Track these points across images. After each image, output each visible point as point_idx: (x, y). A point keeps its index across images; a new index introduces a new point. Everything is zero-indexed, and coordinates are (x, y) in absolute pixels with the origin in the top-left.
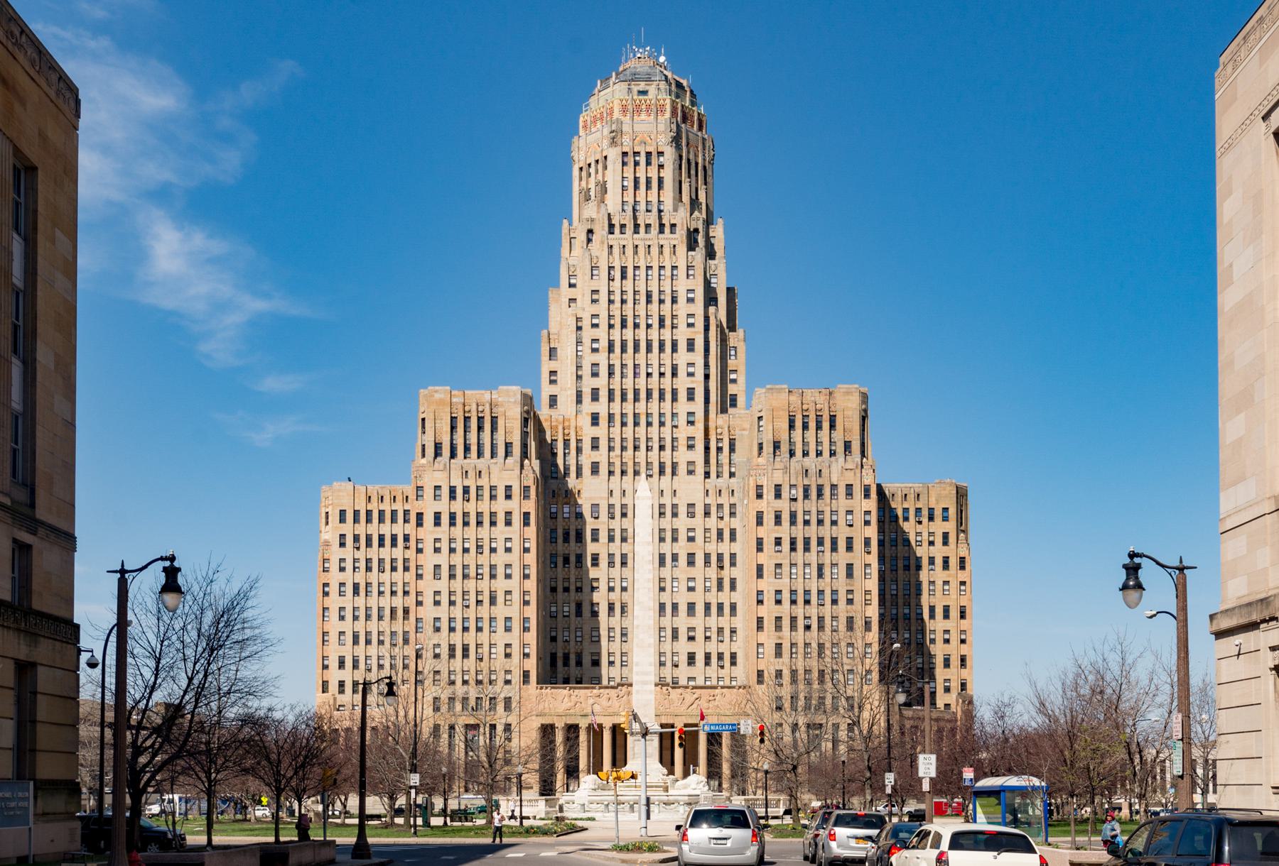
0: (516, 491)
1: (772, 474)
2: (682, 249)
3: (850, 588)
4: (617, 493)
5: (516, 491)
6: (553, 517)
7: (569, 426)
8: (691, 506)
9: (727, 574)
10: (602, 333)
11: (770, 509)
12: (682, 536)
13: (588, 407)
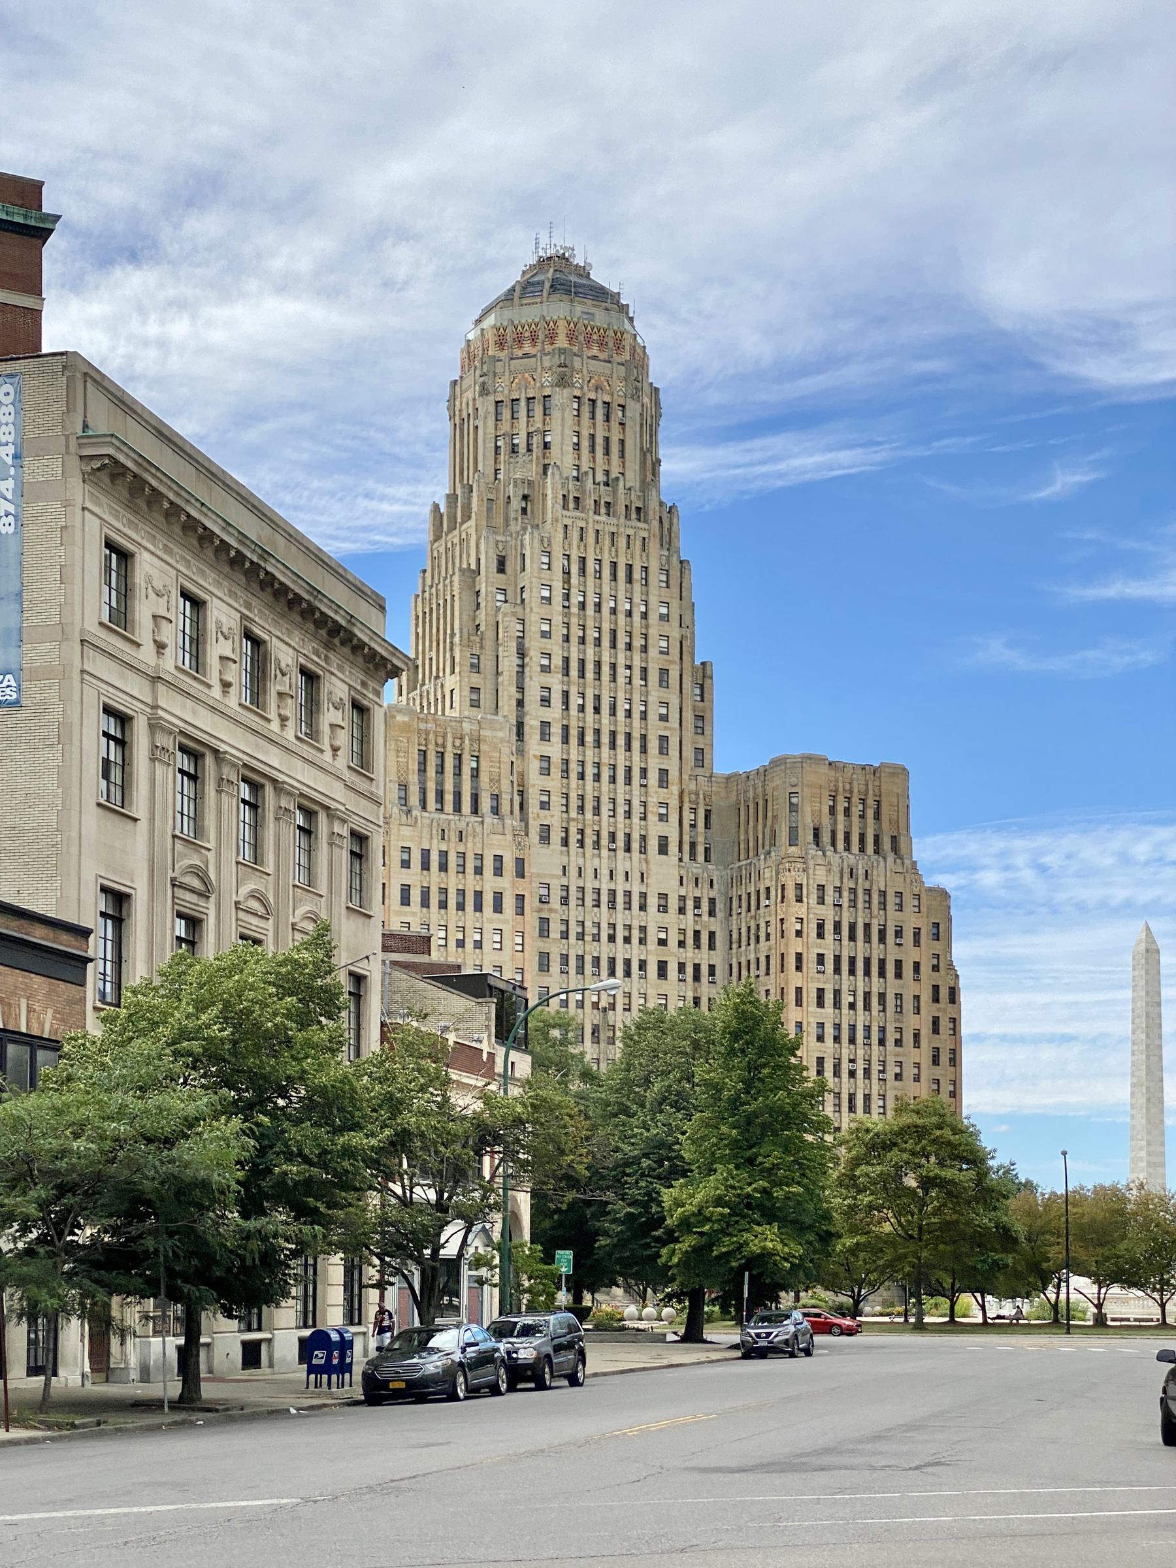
3: (898, 1025)
4: (573, 872)
8: (664, 896)
10: (555, 646)
11: (811, 916)
12: (653, 936)
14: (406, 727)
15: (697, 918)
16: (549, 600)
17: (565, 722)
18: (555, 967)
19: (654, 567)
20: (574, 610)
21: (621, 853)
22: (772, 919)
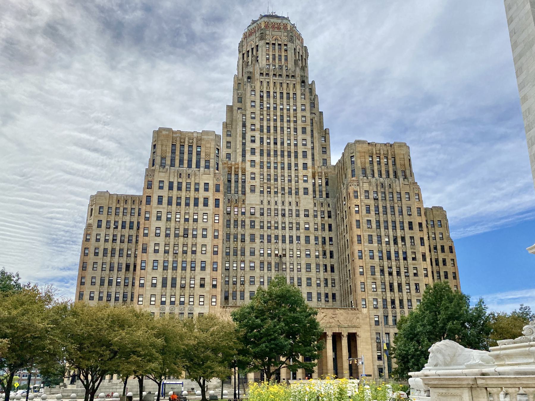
0: (211, 187)
1: (363, 184)
2: (298, 86)
5: (211, 187)
6: (229, 214)
7: (238, 168)
9: (328, 248)
11: (362, 204)
13: (249, 157)
14: (167, 136)
15: (322, 219)
16: (254, 106)
17: (262, 149)
18: (258, 240)
19: (299, 93)
20: (265, 109)
21: (287, 195)
22: (346, 209)
